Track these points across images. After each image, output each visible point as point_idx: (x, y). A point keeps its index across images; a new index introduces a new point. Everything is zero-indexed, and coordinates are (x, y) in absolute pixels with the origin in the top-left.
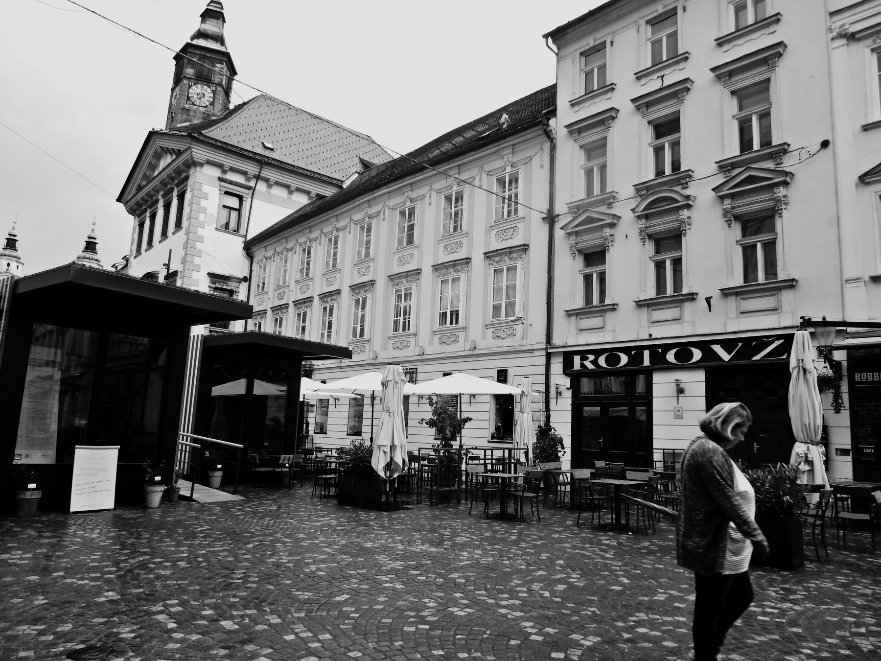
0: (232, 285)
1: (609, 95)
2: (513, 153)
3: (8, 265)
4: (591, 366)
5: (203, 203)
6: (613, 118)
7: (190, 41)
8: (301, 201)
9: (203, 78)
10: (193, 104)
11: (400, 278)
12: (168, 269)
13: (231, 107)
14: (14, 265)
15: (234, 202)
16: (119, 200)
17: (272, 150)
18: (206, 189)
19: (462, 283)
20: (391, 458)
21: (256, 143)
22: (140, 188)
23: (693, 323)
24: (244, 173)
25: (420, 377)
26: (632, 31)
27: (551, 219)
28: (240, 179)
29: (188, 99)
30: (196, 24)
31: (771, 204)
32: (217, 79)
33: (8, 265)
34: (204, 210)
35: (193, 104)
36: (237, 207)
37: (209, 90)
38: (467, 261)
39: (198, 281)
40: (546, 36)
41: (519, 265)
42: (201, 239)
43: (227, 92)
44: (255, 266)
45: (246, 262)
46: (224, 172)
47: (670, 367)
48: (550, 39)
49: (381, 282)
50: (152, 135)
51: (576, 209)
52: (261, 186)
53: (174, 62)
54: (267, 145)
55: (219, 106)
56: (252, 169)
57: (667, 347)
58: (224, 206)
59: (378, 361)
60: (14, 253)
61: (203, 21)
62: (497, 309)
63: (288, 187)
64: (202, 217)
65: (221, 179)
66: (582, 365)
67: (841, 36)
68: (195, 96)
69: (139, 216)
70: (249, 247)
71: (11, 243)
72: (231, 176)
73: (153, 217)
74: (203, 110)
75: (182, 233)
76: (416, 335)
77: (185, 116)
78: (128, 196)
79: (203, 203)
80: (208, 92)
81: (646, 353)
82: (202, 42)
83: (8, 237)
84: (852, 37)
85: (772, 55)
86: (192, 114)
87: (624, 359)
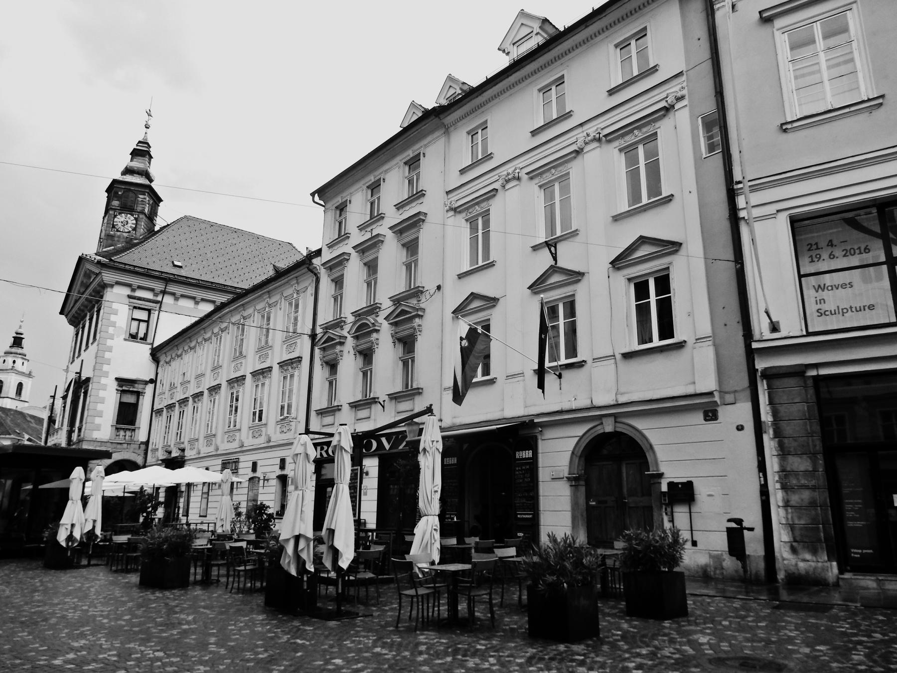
0: (138, 387)
1: (346, 242)
2: (298, 283)
3: (14, 362)
4: (325, 455)
5: (113, 318)
6: (348, 260)
7: (118, 177)
8: (208, 308)
9: (127, 208)
10: (118, 231)
11: (233, 382)
12: (80, 377)
13: (157, 228)
14: (19, 361)
15: (143, 315)
16: (61, 313)
17: (181, 267)
18: (115, 306)
19: (266, 387)
20: (71, 532)
21: (166, 262)
22: (76, 301)
23: (375, 420)
24: (152, 290)
25: (241, 465)
26: (360, 193)
27: (313, 336)
28: (149, 295)
29: (114, 226)
30: (126, 160)
31: (411, 331)
32: (139, 209)
33: (14, 362)
34: (114, 324)
35: (118, 231)
36: (146, 319)
37: (132, 218)
38: (270, 369)
39: (106, 385)
40: (313, 194)
41: (296, 373)
42: (110, 349)
43: (151, 217)
44: (160, 368)
45: (153, 366)
46: (133, 290)
48: (317, 198)
49: (224, 385)
50: (81, 260)
51: (327, 328)
52: (168, 300)
53: (106, 194)
54: (176, 263)
55: (141, 230)
56: (159, 286)
58: (133, 319)
59: (219, 452)
60: (19, 351)
61: (131, 160)
62: (282, 407)
63: (194, 298)
64: (111, 330)
65: (129, 297)
66: (321, 454)
67: (451, 209)
68: (120, 224)
69: (75, 327)
70: (156, 354)
71: (18, 341)
72: (140, 293)
74: (126, 235)
75: (96, 343)
76: (240, 430)
77: (110, 242)
78: (66, 310)
79: (113, 318)
80: (131, 220)
82: (129, 178)
83: (15, 335)
84: (456, 210)
85: (416, 221)
86: (116, 239)
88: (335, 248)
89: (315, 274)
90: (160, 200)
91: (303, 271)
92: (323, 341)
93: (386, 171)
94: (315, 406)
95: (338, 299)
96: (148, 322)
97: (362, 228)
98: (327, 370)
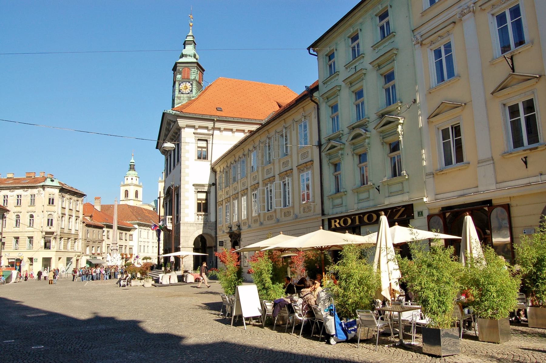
1: (337, 78)
4: (338, 226)
8: (241, 136)
10: (182, 93)
15: (204, 144)
24: (207, 128)
27: (320, 145)
28: (205, 131)
37: (189, 84)
40: (309, 49)
45: (213, 174)
47: (366, 224)
48: (312, 51)
52: (216, 132)
56: (210, 124)
57: (364, 214)
63: (231, 130)
65: (194, 133)
72: (199, 131)
73: (170, 155)
77: (179, 101)
80: (188, 85)
81: (357, 217)
86: (182, 98)
87: (350, 221)
88: (329, 83)
89: (316, 103)
90: (204, 71)
91: (308, 103)
92: (328, 148)
93: (361, 24)
94: (326, 193)
95: (335, 120)
96: (207, 148)
97: (347, 66)
98: (332, 168)
